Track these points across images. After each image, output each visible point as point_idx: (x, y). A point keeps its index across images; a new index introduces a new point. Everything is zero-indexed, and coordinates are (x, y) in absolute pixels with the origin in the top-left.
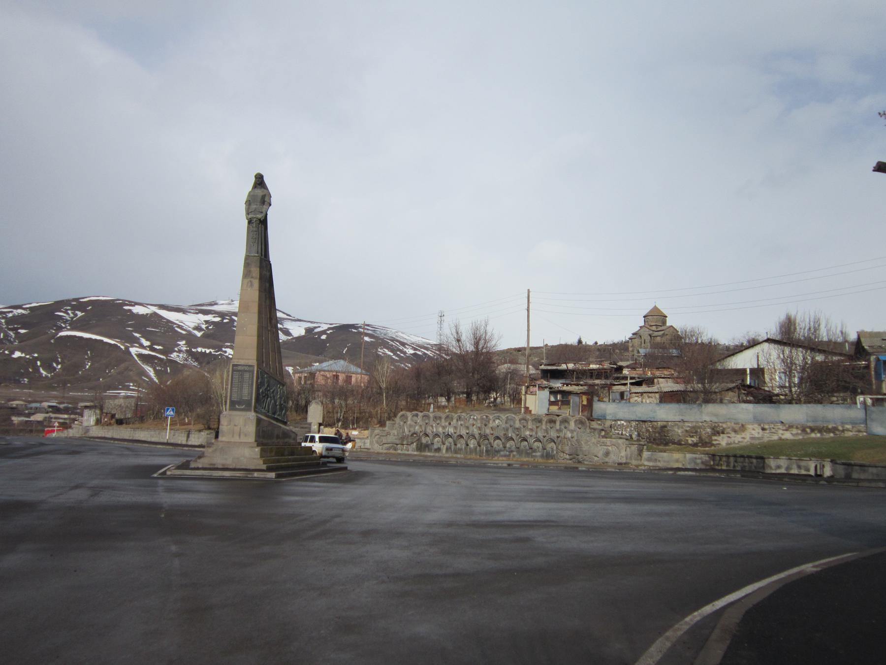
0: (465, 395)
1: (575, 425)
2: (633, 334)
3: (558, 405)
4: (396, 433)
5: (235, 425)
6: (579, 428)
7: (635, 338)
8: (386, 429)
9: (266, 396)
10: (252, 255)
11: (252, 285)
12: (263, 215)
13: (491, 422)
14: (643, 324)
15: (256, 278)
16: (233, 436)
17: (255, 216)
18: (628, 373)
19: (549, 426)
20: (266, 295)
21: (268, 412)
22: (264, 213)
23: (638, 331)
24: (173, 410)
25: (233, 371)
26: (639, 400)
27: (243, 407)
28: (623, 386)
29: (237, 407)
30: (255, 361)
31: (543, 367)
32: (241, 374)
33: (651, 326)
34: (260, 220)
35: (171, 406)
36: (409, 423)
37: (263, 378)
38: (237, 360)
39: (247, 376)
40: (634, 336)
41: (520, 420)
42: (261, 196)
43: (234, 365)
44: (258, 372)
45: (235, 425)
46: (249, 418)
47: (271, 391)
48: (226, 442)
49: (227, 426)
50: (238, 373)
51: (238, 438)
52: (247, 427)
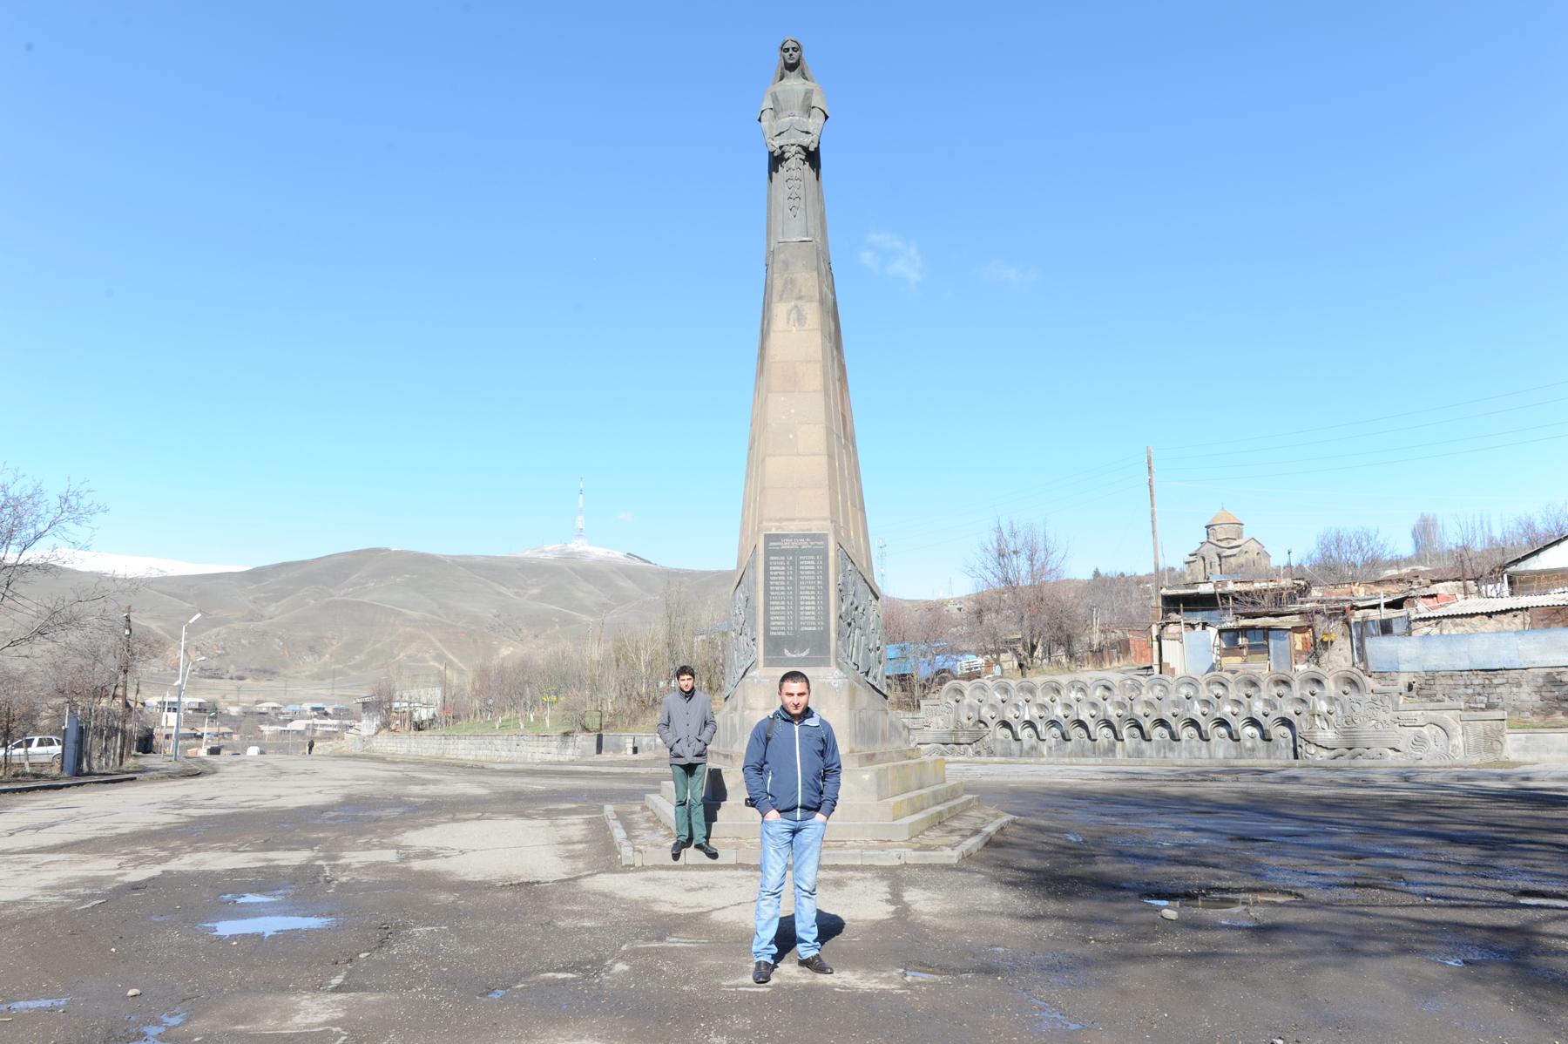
0: (1001, 655)
1: (1337, 687)
2: (1191, 555)
3: (1241, 655)
4: (941, 723)
6: (1344, 693)
8: (921, 714)
10: (795, 240)
11: (801, 319)
12: (815, 138)
14: (1205, 539)
18: (1320, 594)
19: (1275, 690)
23: (1198, 550)
25: (768, 553)
26: (1435, 631)
27: (804, 654)
31: (1164, 591)
33: (1218, 540)
34: (805, 149)
36: (966, 701)
38: (778, 524)
39: (808, 564)
40: (1192, 559)
41: (1208, 684)
42: (803, 94)
43: (768, 538)
46: (829, 684)
50: (783, 558)
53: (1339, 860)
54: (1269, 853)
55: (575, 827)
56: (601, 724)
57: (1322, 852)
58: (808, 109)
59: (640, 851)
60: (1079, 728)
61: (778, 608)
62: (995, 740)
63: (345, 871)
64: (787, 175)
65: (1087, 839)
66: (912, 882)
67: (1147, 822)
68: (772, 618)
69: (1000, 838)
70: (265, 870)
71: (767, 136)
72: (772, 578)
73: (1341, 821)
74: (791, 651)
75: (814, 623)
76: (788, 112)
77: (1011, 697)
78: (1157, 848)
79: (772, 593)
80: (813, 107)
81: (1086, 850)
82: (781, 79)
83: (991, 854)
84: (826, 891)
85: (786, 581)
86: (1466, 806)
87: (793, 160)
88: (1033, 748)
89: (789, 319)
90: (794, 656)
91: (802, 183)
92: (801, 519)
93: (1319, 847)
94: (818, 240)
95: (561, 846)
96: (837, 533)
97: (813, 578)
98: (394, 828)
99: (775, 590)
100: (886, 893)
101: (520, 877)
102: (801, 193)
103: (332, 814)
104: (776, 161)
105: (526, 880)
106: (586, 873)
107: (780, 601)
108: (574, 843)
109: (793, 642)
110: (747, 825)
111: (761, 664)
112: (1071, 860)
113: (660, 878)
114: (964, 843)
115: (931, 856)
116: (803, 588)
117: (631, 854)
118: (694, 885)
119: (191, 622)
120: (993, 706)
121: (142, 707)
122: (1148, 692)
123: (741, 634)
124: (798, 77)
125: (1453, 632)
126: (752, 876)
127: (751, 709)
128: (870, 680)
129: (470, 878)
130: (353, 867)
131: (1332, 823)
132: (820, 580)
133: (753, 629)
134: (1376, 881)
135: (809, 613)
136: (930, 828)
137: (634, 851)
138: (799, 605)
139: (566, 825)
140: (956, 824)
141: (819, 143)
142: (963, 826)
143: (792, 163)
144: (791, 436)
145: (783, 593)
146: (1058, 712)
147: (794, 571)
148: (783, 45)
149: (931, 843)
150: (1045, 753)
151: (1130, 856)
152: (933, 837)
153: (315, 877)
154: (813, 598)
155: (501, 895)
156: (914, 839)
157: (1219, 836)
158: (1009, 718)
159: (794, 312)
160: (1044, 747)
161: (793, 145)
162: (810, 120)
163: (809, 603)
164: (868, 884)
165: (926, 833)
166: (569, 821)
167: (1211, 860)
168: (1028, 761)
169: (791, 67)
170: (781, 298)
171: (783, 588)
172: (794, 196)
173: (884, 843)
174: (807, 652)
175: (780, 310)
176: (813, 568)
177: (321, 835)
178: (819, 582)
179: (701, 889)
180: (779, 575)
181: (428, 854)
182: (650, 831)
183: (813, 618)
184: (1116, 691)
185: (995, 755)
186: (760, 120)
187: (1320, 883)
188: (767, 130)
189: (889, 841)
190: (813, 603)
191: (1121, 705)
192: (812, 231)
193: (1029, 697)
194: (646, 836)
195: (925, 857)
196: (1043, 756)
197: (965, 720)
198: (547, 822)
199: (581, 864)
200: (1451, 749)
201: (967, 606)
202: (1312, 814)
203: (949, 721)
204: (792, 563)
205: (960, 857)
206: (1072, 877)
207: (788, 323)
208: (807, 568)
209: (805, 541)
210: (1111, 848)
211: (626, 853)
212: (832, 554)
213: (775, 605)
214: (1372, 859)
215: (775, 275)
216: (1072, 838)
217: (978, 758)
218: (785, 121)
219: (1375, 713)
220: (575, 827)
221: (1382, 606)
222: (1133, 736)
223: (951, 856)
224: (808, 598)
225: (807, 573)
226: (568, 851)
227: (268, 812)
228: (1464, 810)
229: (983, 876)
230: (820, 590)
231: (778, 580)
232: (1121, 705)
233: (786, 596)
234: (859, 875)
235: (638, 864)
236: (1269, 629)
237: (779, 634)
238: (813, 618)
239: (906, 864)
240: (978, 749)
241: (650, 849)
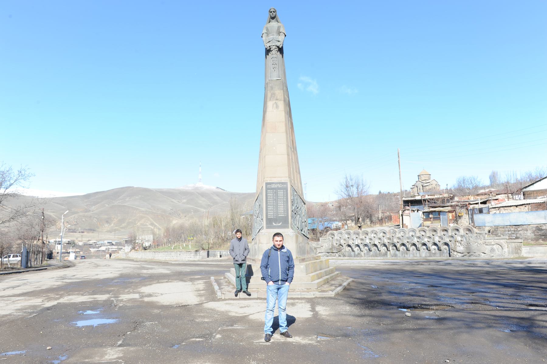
0: (348, 221)
1: (464, 232)
2: (413, 186)
3: (430, 221)
4: (327, 246)
6: (466, 234)
7: (414, 188)
8: (320, 243)
11: (277, 107)
12: (281, 43)
13: (397, 233)
14: (417, 180)
18: (458, 199)
19: (442, 233)
25: (267, 189)
26: (498, 212)
27: (280, 224)
28: (476, 205)
29: (274, 224)
31: (404, 199)
32: (275, 193)
34: (278, 47)
36: (335, 238)
38: (270, 179)
39: (281, 193)
40: (413, 187)
43: (267, 184)
46: (289, 234)
49: (267, 244)
50: (272, 191)
53: (466, 294)
54: (442, 291)
55: (200, 285)
56: (209, 247)
57: (460, 291)
58: (279, 33)
59: (224, 294)
60: (375, 247)
61: (270, 208)
62: (346, 251)
63: (121, 302)
64: (272, 56)
65: (378, 287)
66: (319, 304)
67: (399, 280)
68: (268, 212)
69: (348, 287)
70: (93, 302)
71: (265, 43)
72: (268, 198)
73: (466, 279)
74: (276, 224)
75: (283, 213)
76: (272, 34)
77: (351, 236)
78: (403, 290)
79: (268, 203)
80: (281, 32)
81: (378, 291)
82: (269, 22)
83: (345, 293)
84: (289, 307)
86: (509, 273)
87: (274, 51)
88: (359, 254)
90: (276, 225)
91: (277, 59)
92: (279, 177)
93: (459, 289)
94: (283, 79)
95: (196, 292)
96: (291, 182)
97: (283, 198)
98: (138, 286)
99: (269, 202)
100: (310, 308)
101: (182, 303)
102: (277, 62)
103: (116, 281)
104: (268, 51)
105: (184, 304)
106: (205, 302)
108: (200, 291)
109: (276, 220)
110: (260, 284)
111: (265, 228)
112: (374, 295)
113: (231, 303)
114: (336, 289)
115: (325, 294)
116: (279, 201)
117: (220, 295)
118: (243, 306)
119: (65, 213)
120: (345, 240)
121: (48, 243)
122: (398, 234)
123: (258, 217)
124: (275, 22)
125: (504, 212)
126: (263, 302)
127: (261, 243)
128: (303, 232)
129: (165, 304)
130: (124, 300)
131: (463, 280)
133: (262, 215)
134: (479, 301)
135: (281, 210)
136: (324, 284)
137: (222, 294)
138: (278, 207)
139: (198, 284)
140: (333, 282)
141: (283, 45)
142: (336, 283)
143: (273, 52)
145: (272, 203)
146: (367, 241)
147: (276, 195)
148: (270, 10)
149: (325, 289)
150: (363, 255)
151: (394, 293)
152: (326, 287)
153: (111, 304)
154: (283, 205)
155: (176, 310)
156: (319, 288)
157: (424, 285)
158: (350, 243)
160: (362, 254)
161: (274, 46)
162: (280, 37)
163: (281, 206)
164: (303, 304)
165: (323, 286)
166: (198, 283)
167: (422, 294)
168: (357, 258)
169: (273, 18)
170: (270, 100)
171: (272, 201)
172: (274, 64)
173: (309, 290)
174: (281, 223)
175: (270, 104)
176: (283, 194)
177: (112, 289)
178: (285, 199)
179: (245, 307)
181: (150, 295)
182: (227, 286)
183: (283, 212)
184: (387, 234)
185: (346, 257)
186: (262, 37)
187: (460, 302)
188: (265, 41)
189: (310, 289)
190: (283, 206)
191: (389, 239)
192: (281, 76)
193: (357, 236)
194: (226, 288)
195: (323, 294)
196: (362, 257)
197: (335, 245)
198: (191, 283)
199: (203, 298)
200: (503, 253)
201: (336, 204)
202: (456, 277)
203: (330, 244)
204: (275, 193)
205: (335, 294)
206: (374, 301)
207: (273, 108)
208: (280, 194)
210: (387, 290)
211: (219, 294)
212: (289, 189)
213: (269, 207)
214: (477, 293)
215: (268, 92)
216: (373, 286)
217: (340, 258)
218: (271, 37)
219: (477, 240)
220: (200, 285)
221: (479, 203)
222: (393, 249)
223: (332, 294)
224: (281, 205)
225: (281, 196)
226: (199, 294)
227: (93, 281)
228: (509, 275)
229: (343, 301)
230: (285, 202)
231: (270, 199)
232: (389, 239)
234: (300, 301)
235: (223, 298)
236: (440, 212)
237: (271, 217)
239: (316, 297)
240: (340, 255)
241: (227, 293)
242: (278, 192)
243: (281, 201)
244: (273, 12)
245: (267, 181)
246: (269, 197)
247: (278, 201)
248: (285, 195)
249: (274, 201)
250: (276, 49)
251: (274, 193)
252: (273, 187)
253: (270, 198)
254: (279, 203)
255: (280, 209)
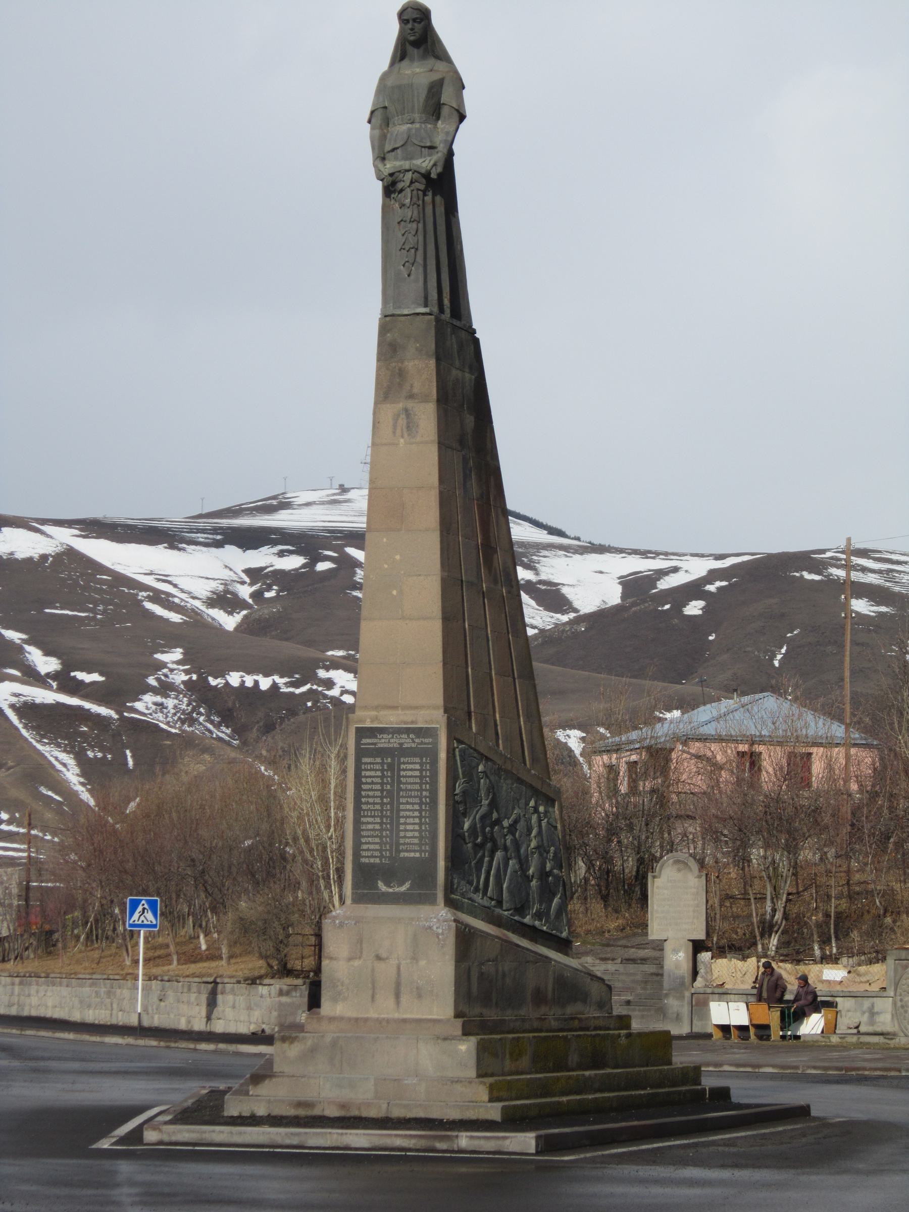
5: (379, 958)
9: (489, 845)
10: (406, 312)
11: (411, 427)
12: (438, 156)
15: (425, 399)
16: (373, 997)
17: (406, 165)
20: (465, 461)
21: (500, 903)
22: (442, 148)
24: (153, 905)
25: (360, 753)
27: (403, 889)
29: (382, 887)
30: (442, 711)
32: (391, 767)
34: (426, 176)
35: (145, 893)
37: (470, 774)
38: (374, 713)
39: (411, 769)
43: (362, 732)
44: (451, 752)
45: (379, 958)
46: (430, 928)
47: (506, 823)
48: (350, 1019)
49: (350, 959)
50: (379, 760)
51: (391, 1002)
52: (423, 963)
61: (370, 827)
68: (363, 840)
75: (417, 848)
79: (364, 807)
85: (382, 791)
89: (395, 427)
90: (391, 890)
97: (417, 787)
99: (367, 803)
107: (374, 817)
109: (390, 873)
127: (331, 958)
132: (426, 790)
135: (410, 834)
138: (398, 824)
144: (395, 592)
147: (392, 777)
154: (417, 814)
159: (404, 416)
171: (378, 800)
174: (407, 885)
176: (417, 773)
178: (424, 793)
180: (372, 783)
183: (416, 841)
190: (417, 821)
204: (391, 767)
207: (394, 433)
208: (409, 773)
209: (408, 736)
213: (368, 823)
224: (411, 814)
230: (426, 804)
233: (382, 811)
237: (372, 860)
238: (416, 841)
242: (402, 766)
243: (410, 800)
244: (411, 22)
245: (363, 721)
246: (367, 783)
247: (401, 800)
248: (426, 777)
249: (385, 800)
250: (417, 185)
251: (385, 768)
252: (382, 746)
253: (369, 787)
254: (402, 807)
255: (406, 830)
